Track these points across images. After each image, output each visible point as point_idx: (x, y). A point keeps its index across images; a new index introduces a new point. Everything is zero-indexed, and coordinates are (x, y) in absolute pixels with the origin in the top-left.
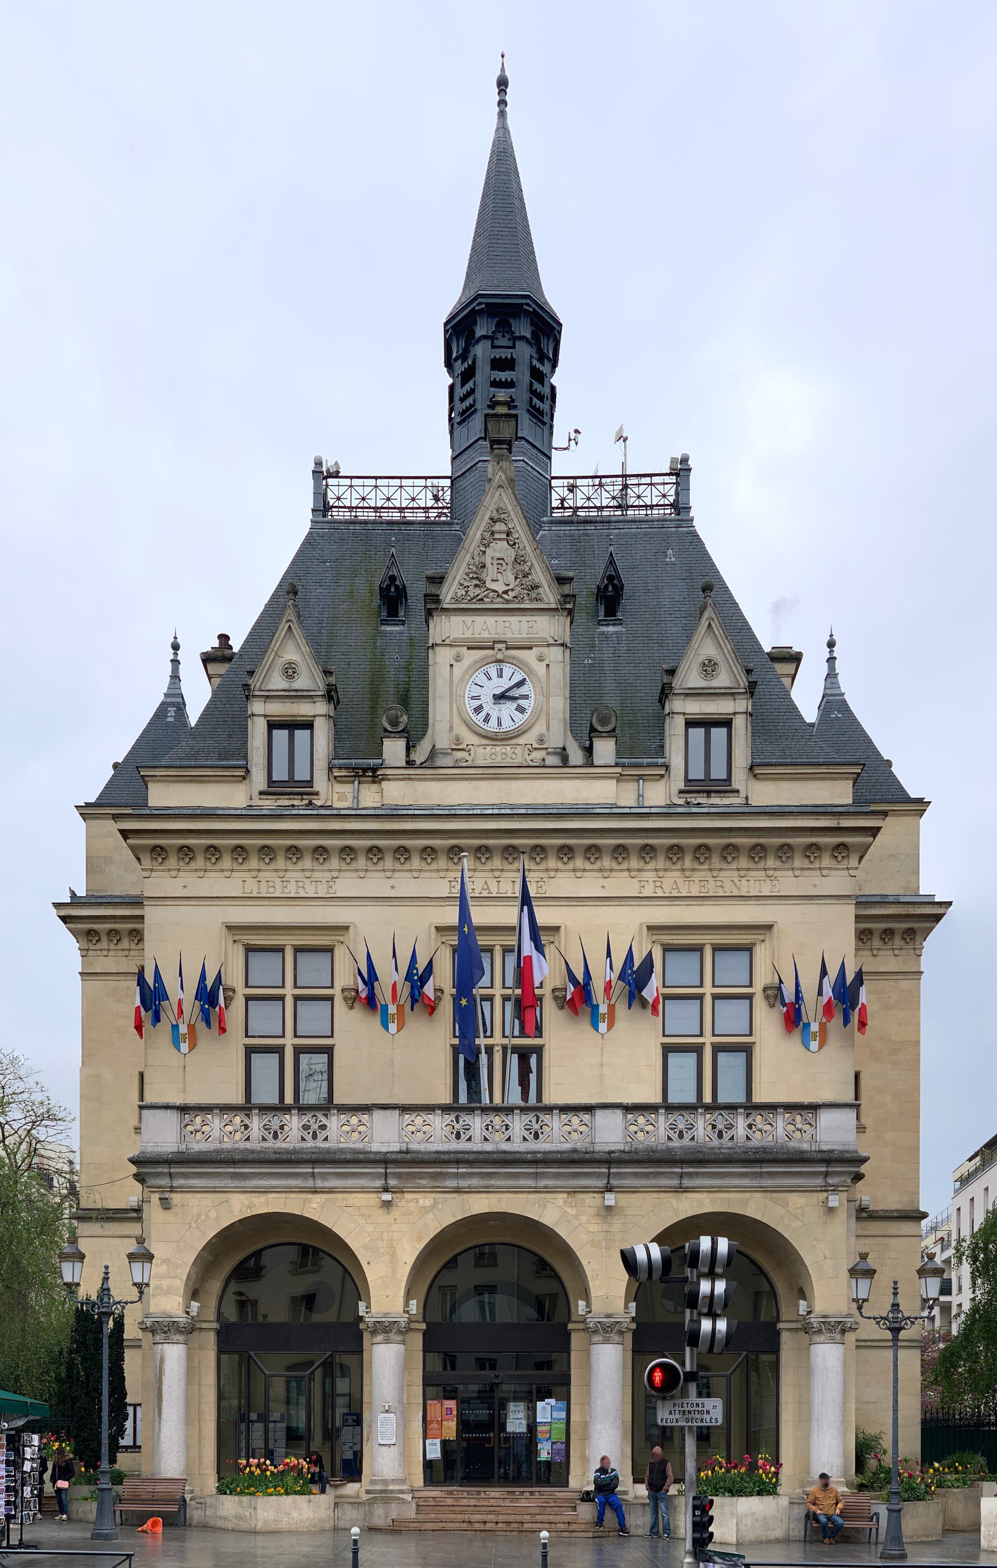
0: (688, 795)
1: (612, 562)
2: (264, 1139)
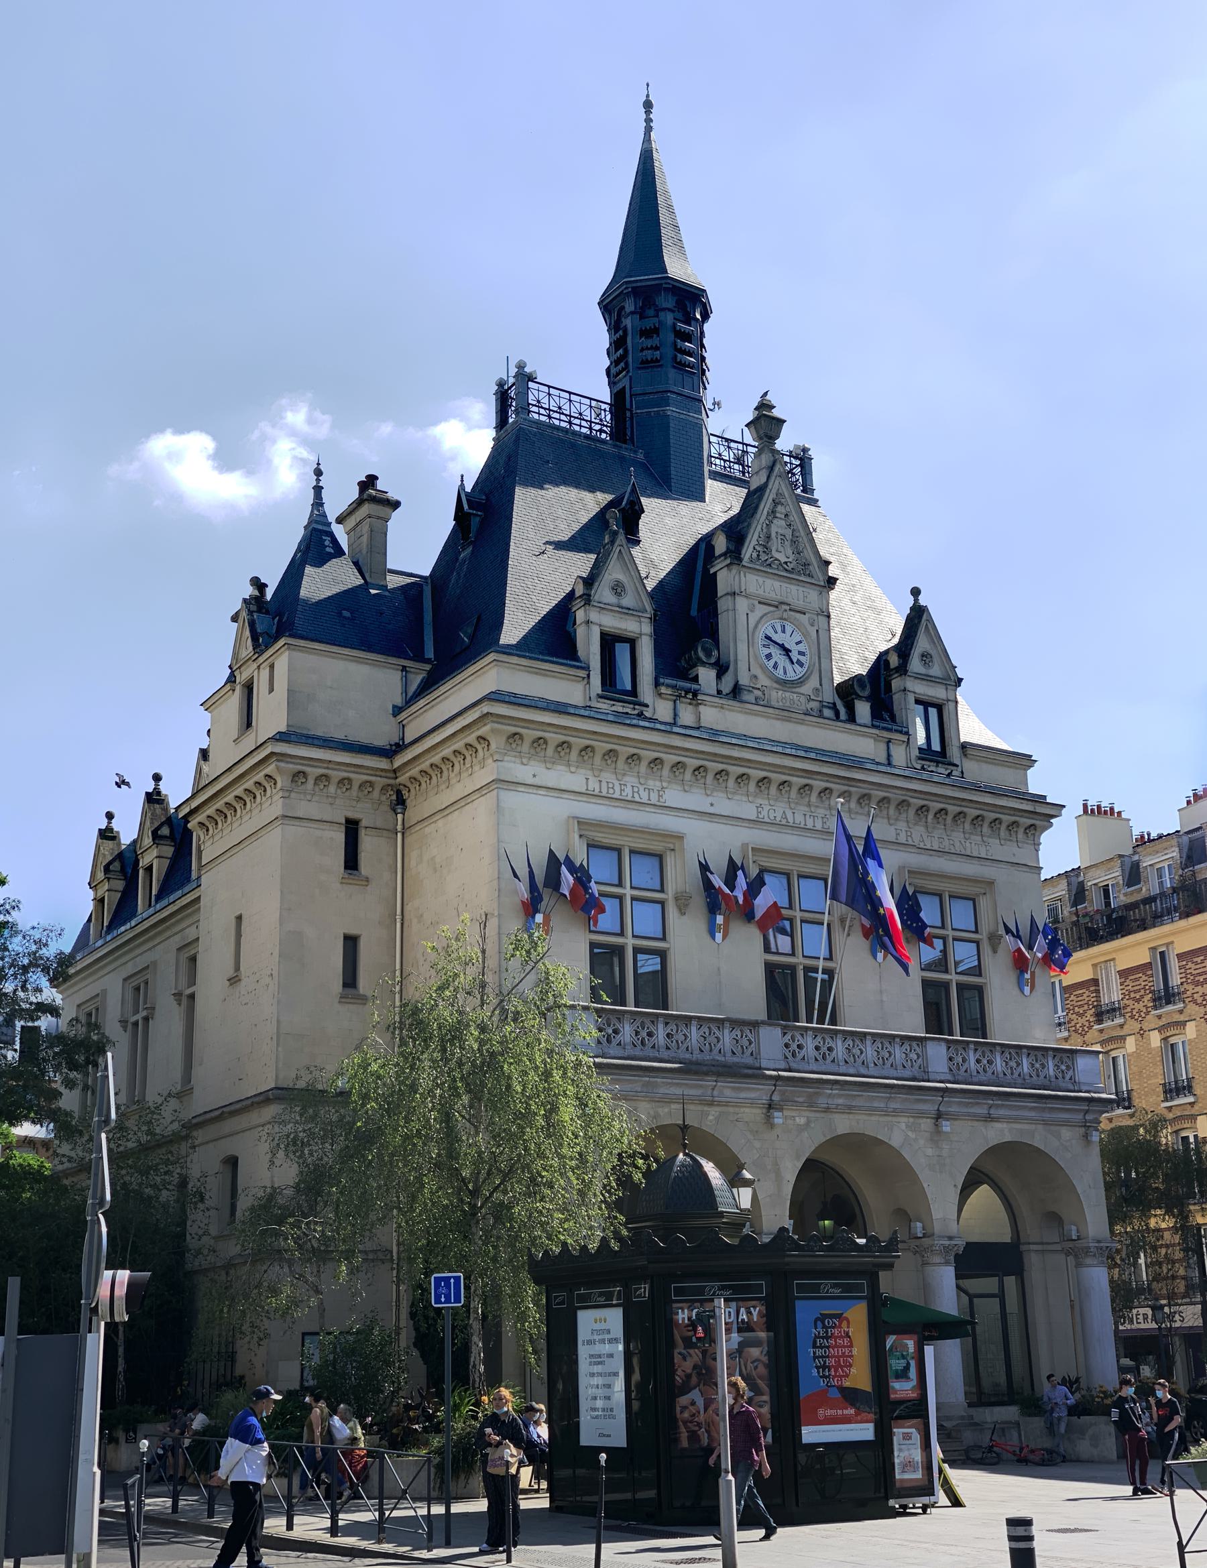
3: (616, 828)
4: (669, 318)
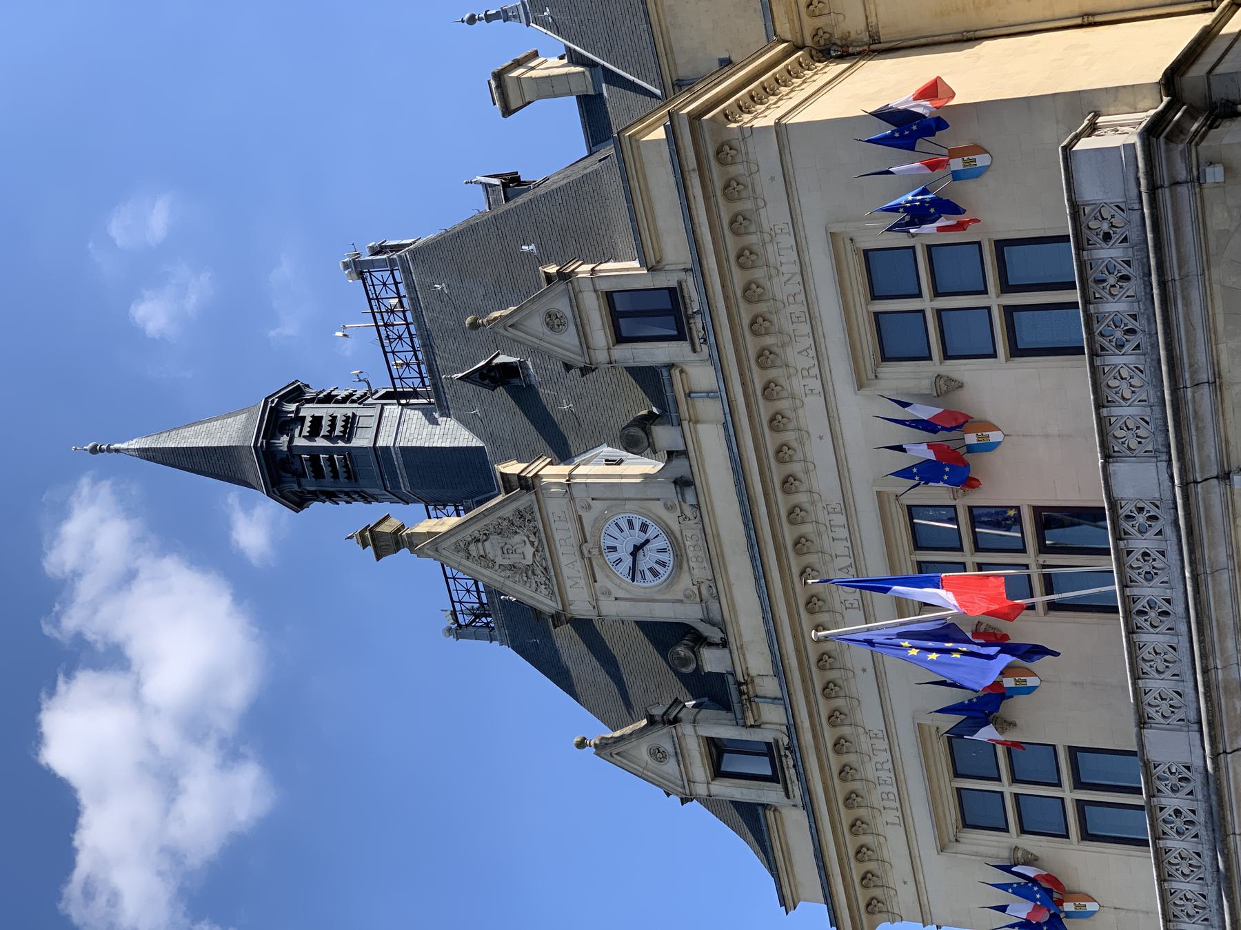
0: (697, 341)
3: (933, 798)
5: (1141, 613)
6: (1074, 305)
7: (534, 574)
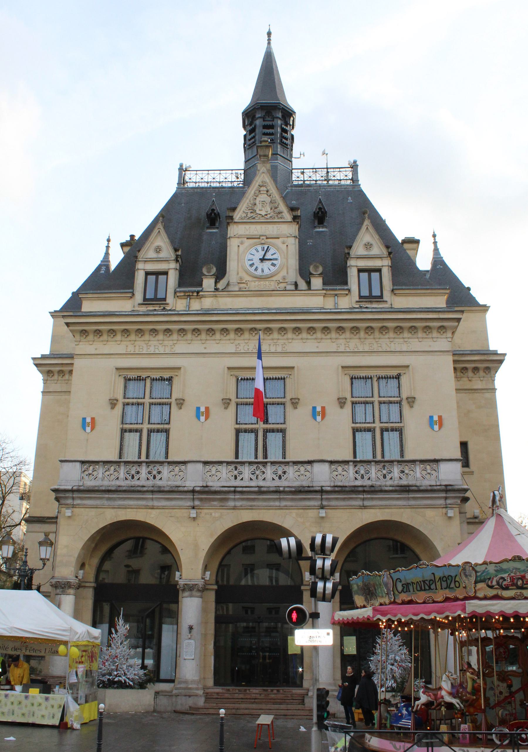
1: (320, 202)
2: (126, 479)
4: (279, 122)
5: (236, 468)
6: (256, 457)
7: (251, 212)
